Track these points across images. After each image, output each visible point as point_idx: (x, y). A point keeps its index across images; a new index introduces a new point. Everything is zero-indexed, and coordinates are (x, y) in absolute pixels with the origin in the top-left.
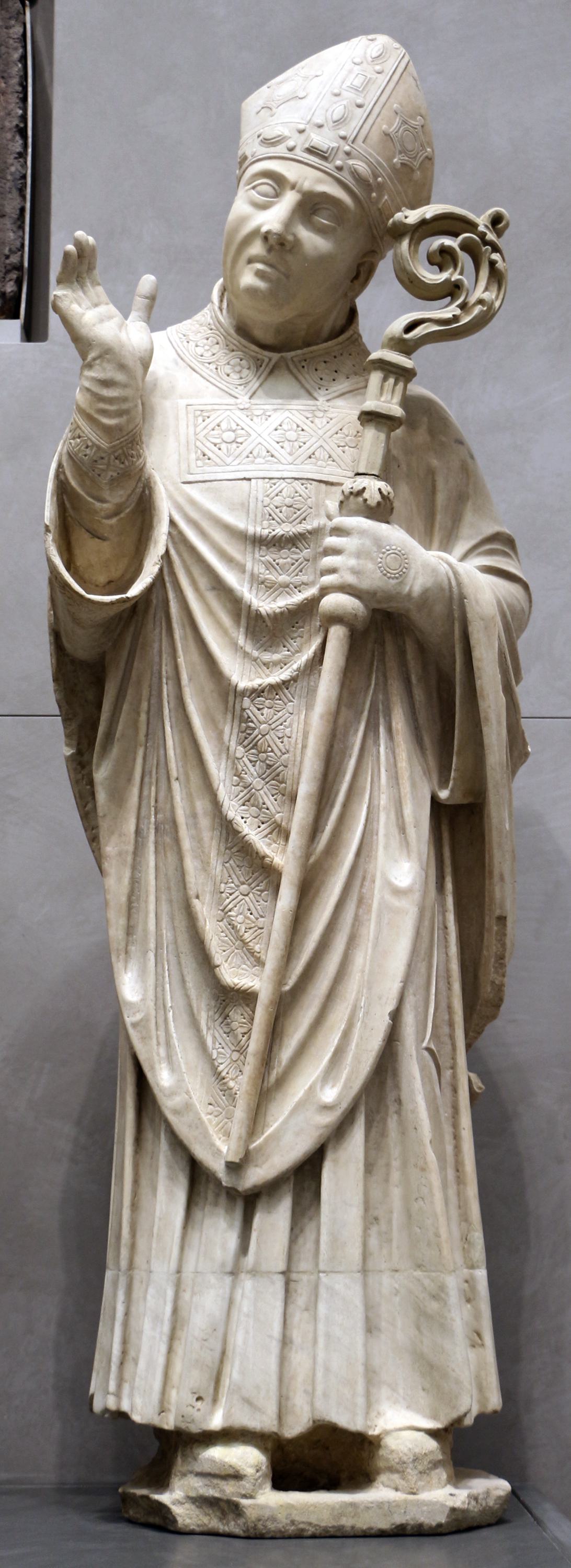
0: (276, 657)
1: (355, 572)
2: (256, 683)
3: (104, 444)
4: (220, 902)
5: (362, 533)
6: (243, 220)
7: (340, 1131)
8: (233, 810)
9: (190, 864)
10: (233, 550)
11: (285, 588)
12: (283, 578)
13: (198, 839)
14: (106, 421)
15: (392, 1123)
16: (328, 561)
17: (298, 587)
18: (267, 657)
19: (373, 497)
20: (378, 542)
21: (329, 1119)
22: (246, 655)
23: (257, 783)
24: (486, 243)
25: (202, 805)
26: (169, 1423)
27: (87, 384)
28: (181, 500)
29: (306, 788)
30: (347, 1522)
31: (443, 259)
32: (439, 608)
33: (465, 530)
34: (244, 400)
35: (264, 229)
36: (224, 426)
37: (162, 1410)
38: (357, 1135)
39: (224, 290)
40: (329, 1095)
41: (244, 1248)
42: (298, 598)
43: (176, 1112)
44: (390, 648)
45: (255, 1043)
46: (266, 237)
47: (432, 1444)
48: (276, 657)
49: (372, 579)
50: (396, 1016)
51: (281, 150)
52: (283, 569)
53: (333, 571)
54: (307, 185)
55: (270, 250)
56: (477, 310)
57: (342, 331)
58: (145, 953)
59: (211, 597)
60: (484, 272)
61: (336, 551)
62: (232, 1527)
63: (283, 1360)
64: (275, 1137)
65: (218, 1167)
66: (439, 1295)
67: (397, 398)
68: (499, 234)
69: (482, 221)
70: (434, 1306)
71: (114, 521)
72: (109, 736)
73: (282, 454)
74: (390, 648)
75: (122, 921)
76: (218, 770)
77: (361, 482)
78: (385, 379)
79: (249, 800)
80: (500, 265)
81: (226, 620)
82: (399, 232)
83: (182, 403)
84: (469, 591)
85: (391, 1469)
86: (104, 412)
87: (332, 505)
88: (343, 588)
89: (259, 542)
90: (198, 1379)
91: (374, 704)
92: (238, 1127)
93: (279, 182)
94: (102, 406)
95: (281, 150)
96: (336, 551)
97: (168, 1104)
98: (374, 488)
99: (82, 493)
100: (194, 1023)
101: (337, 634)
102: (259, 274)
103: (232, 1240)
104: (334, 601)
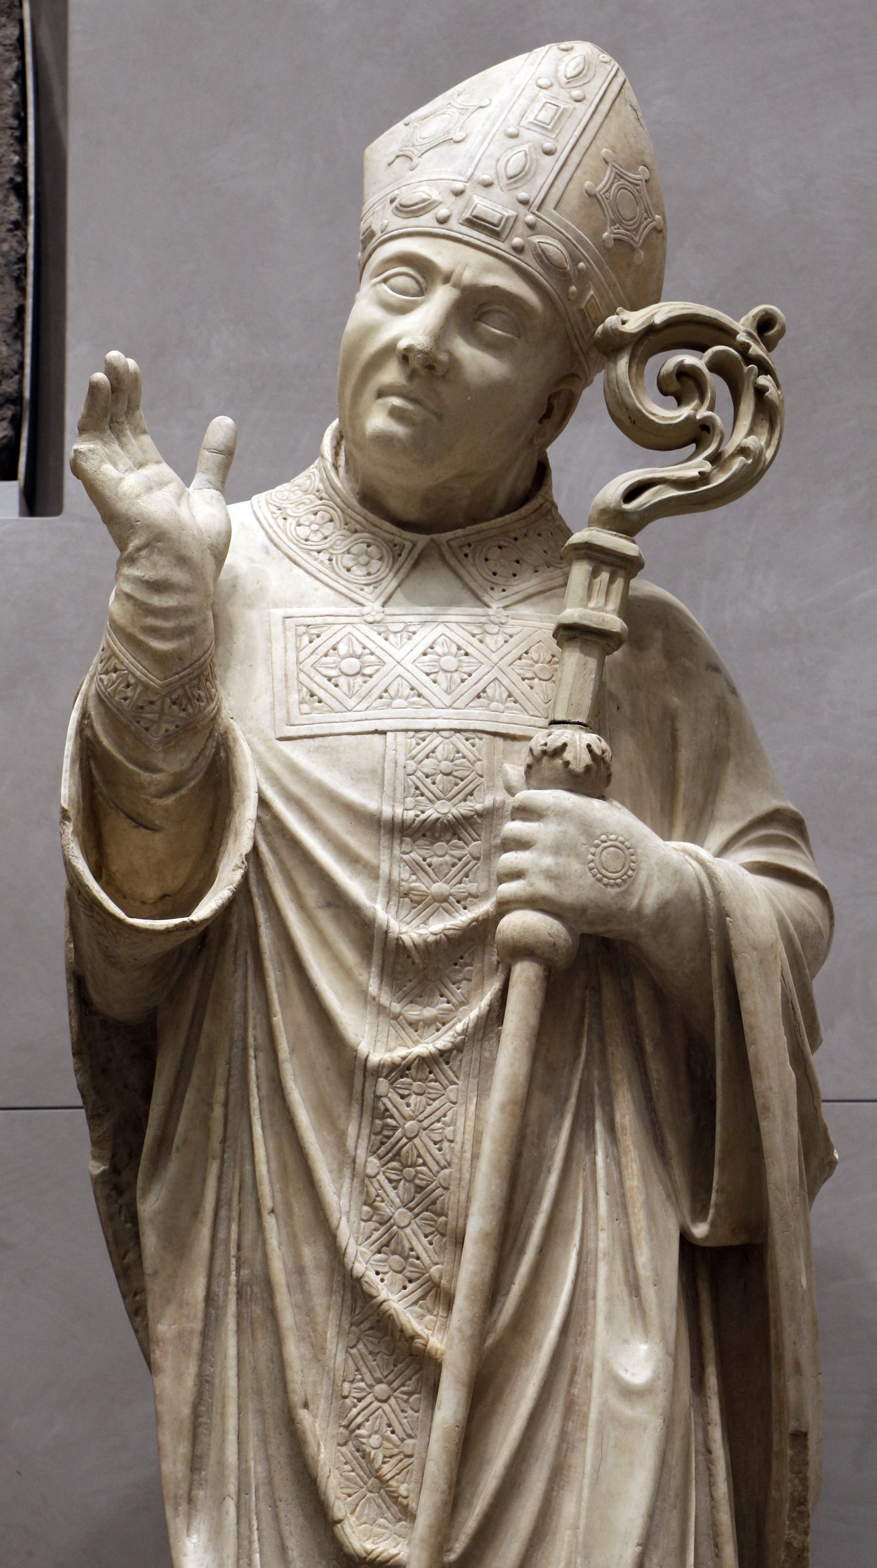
0: (429, 1012)
1: (551, 876)
2: (398, 1053)
3: (155, 681)
4: (342, 1412)
5: (562, 814)
6: (370, 330)
9: (294, 1350)
12: (439, 887)
13: (306, 1310)
14: (158, 645)
16: (510, 859)
17: (463, 901)
18: (414, 1012)
20: (587, 828)
22: (381, 1010)
23: (401, 1216)
24: (749, 359)
27: (127, 588)
28: (276, 766)
32: (686, 932)
33: (724, 807)
34: (373, 608)
35: (402, 344)
36: (343, 649)
39: (340, 438)
42: (463, 918)
44: (609, 996)
46: (405, 356)
48: (429, 1012)
51: (427, 222)
52: (438, 873)
53: (517, 875)
54: (468, 277)
55: (412, 376)
56: (737, 463)
57: (526, 498)
58: (220, 1502)
59: (324, 918)
60: (748, 406)
61: (522, 844)
67: (614, 603)
68: (770, 346)
71: (170, 800)
72: (164, 1143)
73: (435, 692)
74: (609, 996)
75: (184, 1448)
78: (595, 574)
80: (773, 393)
81: (350, 955)
83: (279, 613)
84: (733, 904)
86: (154, 631)
87: (515, 771)
88: (534, 903)
91: (585, 1085)
94: (151, 621)
95: (427, 222)
96: (522, 844)
99: (120, 757)
102: (395, 414)
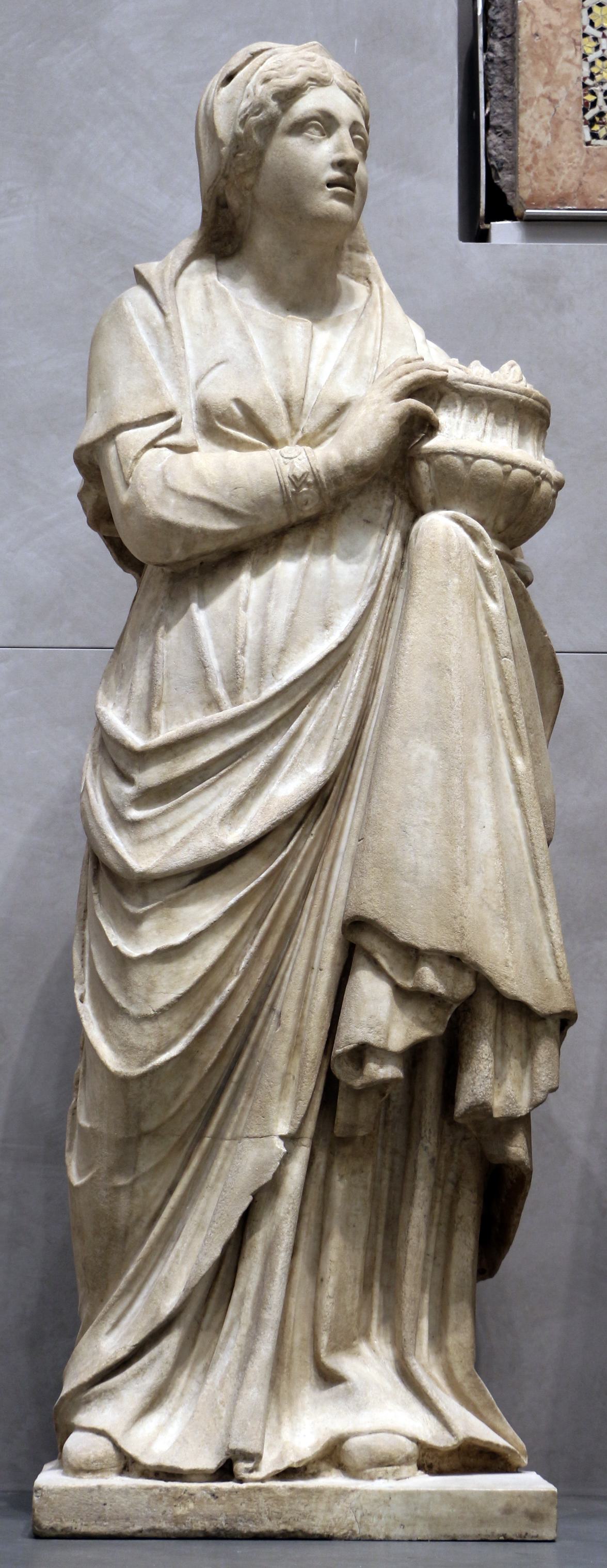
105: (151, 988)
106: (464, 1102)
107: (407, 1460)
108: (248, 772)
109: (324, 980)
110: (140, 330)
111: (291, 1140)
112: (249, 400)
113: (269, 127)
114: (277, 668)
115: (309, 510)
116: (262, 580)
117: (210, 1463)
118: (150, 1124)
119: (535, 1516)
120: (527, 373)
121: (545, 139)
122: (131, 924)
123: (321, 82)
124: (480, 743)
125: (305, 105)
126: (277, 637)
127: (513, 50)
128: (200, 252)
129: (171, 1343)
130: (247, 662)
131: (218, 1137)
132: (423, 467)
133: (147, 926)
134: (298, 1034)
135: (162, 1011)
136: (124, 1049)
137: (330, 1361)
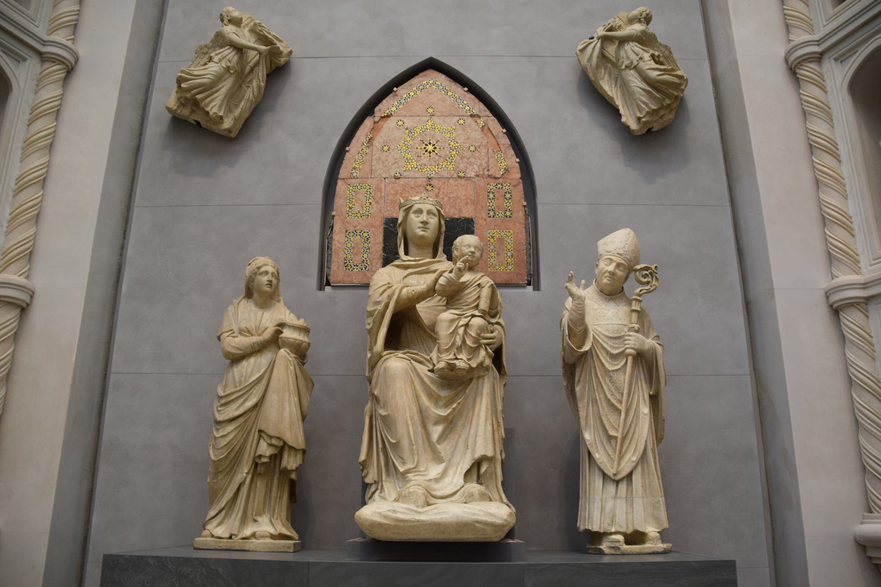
0: (616, 363)
1: (634, 344)
2: (613, 369)
4: (607, 417)
5: (635, 336)
6: (603, 268)
7: (636, 467)
8: (609, 397)
9: (600, 408)
10: (606, 340)
11: (618, 348)
12: (617, 346)
13: (601, 403)
14: (579, 312)
15: (645, 465)
16: (627, 342)
17: (620, 348)
18: (614, 363)
19: (637, 328)
21: (634, 464)
22: (609, 363)
23: (614, 391)
24: (654, 272)
25: (602, 396)
26: (602, 531)
27: (575, 304)
28: (593, 329)
29: (625, 392)
30: (643, 551)
31: (645, 276)
32: (651, 352)
34: (604, 307)
35: (609, 270)
36: (601, 312)
37: (600, 528)
38: (639, 468)
39: (596, 281)
40: (634, 459)
41: (616, 493)
42: (620, 350)
43: (601, 463)
44: (639, 360)
45: (618, 447)
46: (609, 272)
47: (658, 535)
48: (616, 363)
49: (638, 346)
50: (646, 441)
51: (611, 253)
52: (617, 344)
53: (628, 344)
54: (618, 261)
55: (611, 275)
56: (654, 287)
58: (591, 428)
59: (601, 350)
60: (654, 279)
61: (629, 340)
62: (618, 552)
63: (626, 517)
64: (623, 468)
65: (611, 475)
66: (658, 502)
67: (639, 307)
68: (656, 270)
69: (653, 267)
70: (657, 505)
71: (579, 333)
72: (579, 381)
73: (614, 318)
75: (585, 422)
76: (605, 388)
77: (633, 325)
78: (636, 303)
79: (612, 395)
80: (658, 277)
81: (605, 355)
82: (636, 270)
83: (591, 307)
85: (650, 540)
86: (578, 310)
87: (626, 330)
88: (631, 348)
89: (611, 338)
90: (608, 521)
91: (637, 375)
92: (615, 467)
93: (611, 260)
94: (578, 309)
95: (611, 253)
96: (629, 340)
97: (598, 462)
98: (636, 326)
99: (573, 327)
100: (602, 443)
101: (630, 358)
102: (608, 280)
103: (614, 491)
104: (628, 351)
105: (220, 443)
106: (282, 466)
107: (267, 537)
108: (241, 400)
109: (255, 442)
110: (230, 313)
111: (247, 473)
112: (248, 327)
113: (255, 274)
114: (248, 380)
115: (257, 349)
116: (247, 363)
117: (227, 536)
118: (220, 470)
119: (289, 548)
120: (305, 321)
121: (336, 270)
122: (218, 430)
123: (266, 265)
124: (287, 396)
125: (262, 270)
126: (248, 374)
127: (331, 251)
128: (244, 298)
129: (223, 513)
130: (243, 379)
131: (234, 473)
132: (280, 340)
133: (220, 431)
134: (250, 453)
135: (221, 448)
136: (215, 455)
137: (255, 518)
